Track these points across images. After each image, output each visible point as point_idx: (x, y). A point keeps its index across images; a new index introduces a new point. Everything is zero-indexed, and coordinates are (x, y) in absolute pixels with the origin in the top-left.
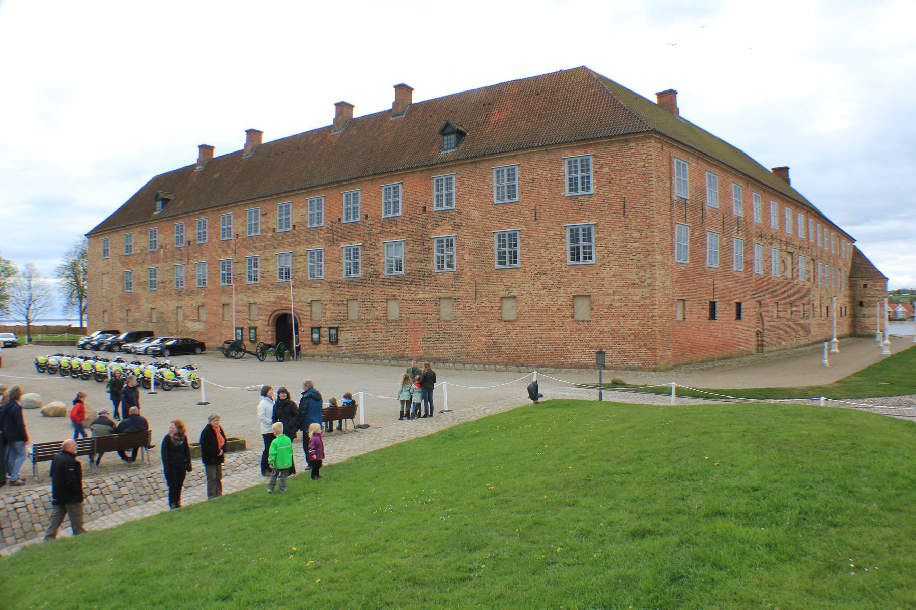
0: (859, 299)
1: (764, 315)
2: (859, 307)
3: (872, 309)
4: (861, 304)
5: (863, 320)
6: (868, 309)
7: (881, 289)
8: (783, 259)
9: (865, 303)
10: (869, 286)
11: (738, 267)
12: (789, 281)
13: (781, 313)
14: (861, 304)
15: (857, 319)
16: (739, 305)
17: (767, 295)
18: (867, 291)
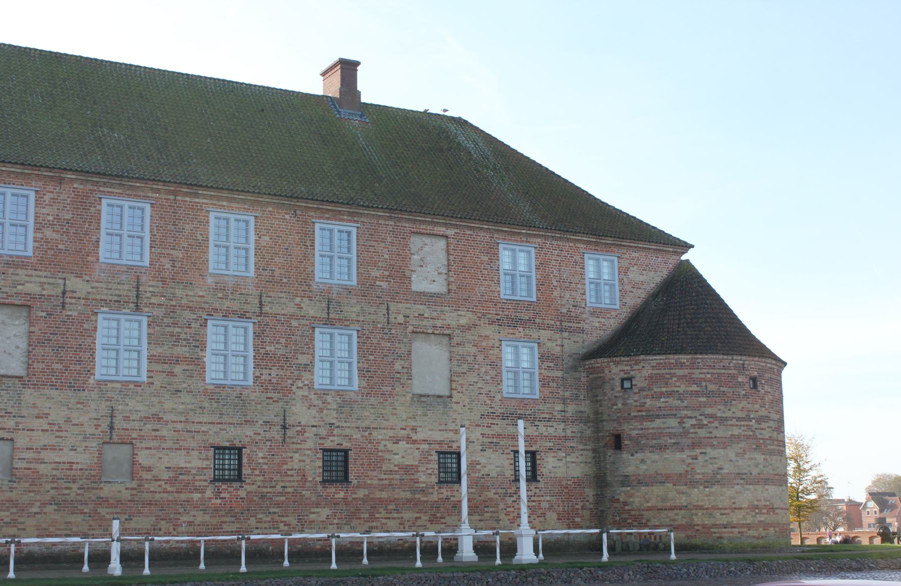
0: (610, 427)
2: (610, 452)
3: (655, 457)
4: (617, 442)
5: (621, 493)
6: (639, 456)
7: (694, 388)
9: (631, 438)
10: (639, 382)
14: (617, 442)
15: (608, 493)
18: (633, 400)
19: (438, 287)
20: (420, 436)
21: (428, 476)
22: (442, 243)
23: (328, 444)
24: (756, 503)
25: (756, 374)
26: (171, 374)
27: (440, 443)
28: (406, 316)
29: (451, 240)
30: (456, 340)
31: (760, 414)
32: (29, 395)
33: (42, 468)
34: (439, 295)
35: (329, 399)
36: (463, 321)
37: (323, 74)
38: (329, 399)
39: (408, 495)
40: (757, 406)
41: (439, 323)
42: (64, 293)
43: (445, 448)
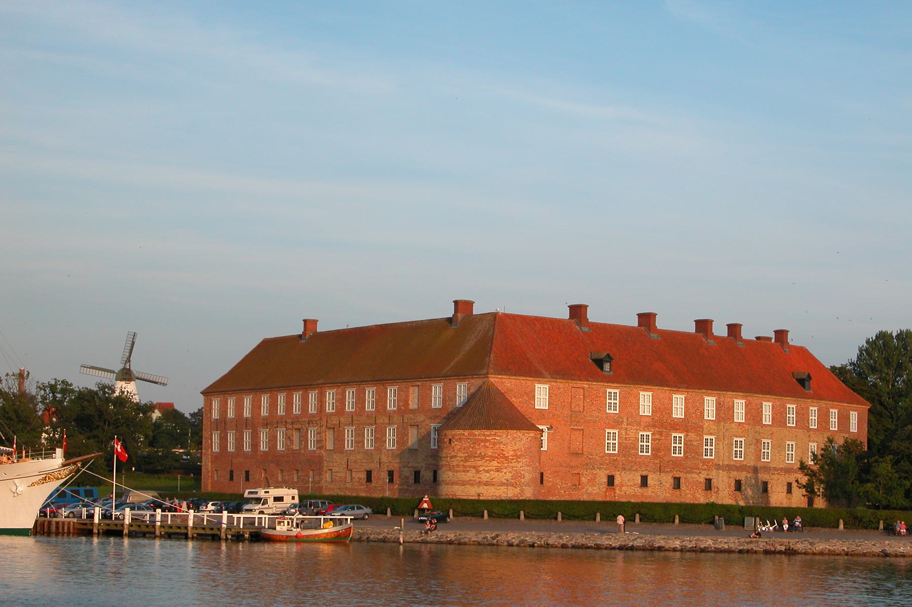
1: (269, 479)
8: (289, 435)
11: (247, 448)
12: (295, 452)
13: (287, 477)
16: (247, 473)
17: (271, 465)
19: (416, 407)
20: (410, 465)
21: (412, 481)
22: (416, 388)
23: (389, 469)
24: (447, 493)
25: (451, 437)
26: (358, 446)
27: (415, 468)
28: (408, 419)
29: (420, 387)
30: (420, 427)
31: (452, 455)
32: (335, 456)
33: (337, 478)
34: (415, 410)
35: (389, 452)
36: (422, 419)
37: (204, 393)
38: (389, 452)
39: (406, 487)
40: (450, 451)
41: (416, 421)
42: (339, 423)
43: (416, 470)
